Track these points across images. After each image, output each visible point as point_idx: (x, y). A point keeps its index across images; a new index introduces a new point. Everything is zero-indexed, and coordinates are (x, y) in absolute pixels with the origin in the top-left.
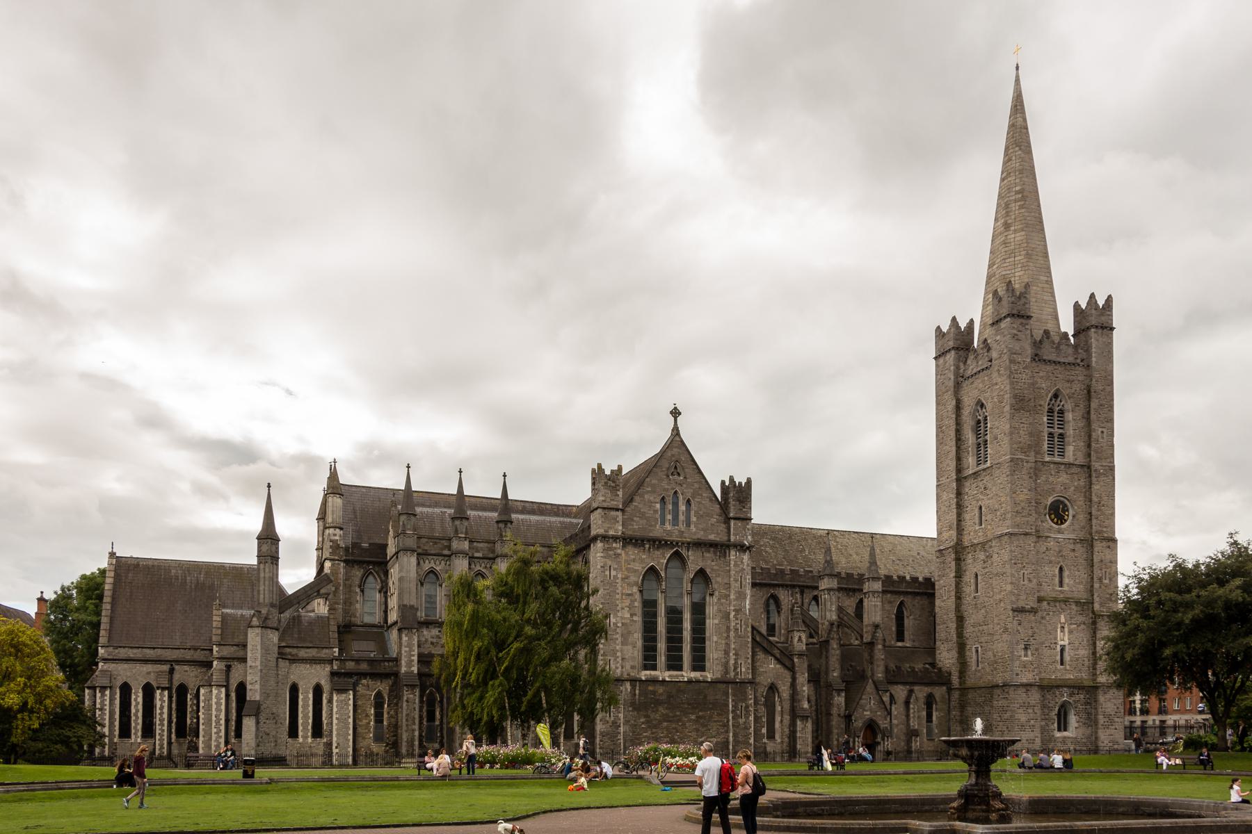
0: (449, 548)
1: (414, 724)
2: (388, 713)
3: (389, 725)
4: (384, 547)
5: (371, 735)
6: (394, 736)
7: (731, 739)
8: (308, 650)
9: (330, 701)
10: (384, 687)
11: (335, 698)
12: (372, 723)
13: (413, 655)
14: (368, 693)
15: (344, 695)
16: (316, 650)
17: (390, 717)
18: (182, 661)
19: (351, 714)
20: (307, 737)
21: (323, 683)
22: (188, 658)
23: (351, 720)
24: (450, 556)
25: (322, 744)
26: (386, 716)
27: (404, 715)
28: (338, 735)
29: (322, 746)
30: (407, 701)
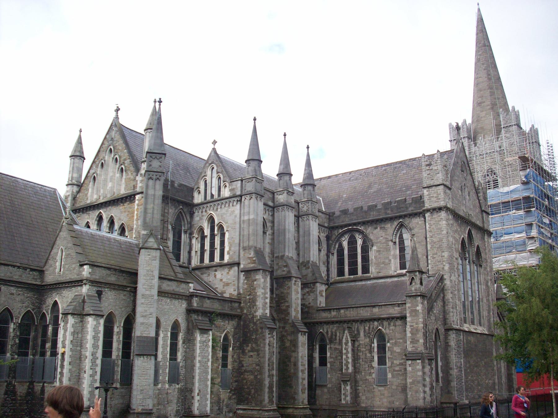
0: (273, 199)
1: (273, 369)
2: (233, 357)
3: (233, 368)
4: (190, 191)
5: (219, 380)
6: (236, 381)
7: (497, 381)
8: (170, 283)
9: (189, 341)
10: (229, 327)
11: (198, 337)
12: (220, 367)
13: (267, 298)
14: (218, 334)
15: (206, 336)
16: (175, 283)
17: (234, 361)
18: (9, 281)
19: (210, 357)
20: (164, 383)
21: (180, 320)
22: (16, 278)
23: (210, 364)
24: (273, 208)
25: (176, 390)
26: (230, 359)
27: (267, 359)
28: (200, 380)
29: (176, 393)
30: (269, 345)
